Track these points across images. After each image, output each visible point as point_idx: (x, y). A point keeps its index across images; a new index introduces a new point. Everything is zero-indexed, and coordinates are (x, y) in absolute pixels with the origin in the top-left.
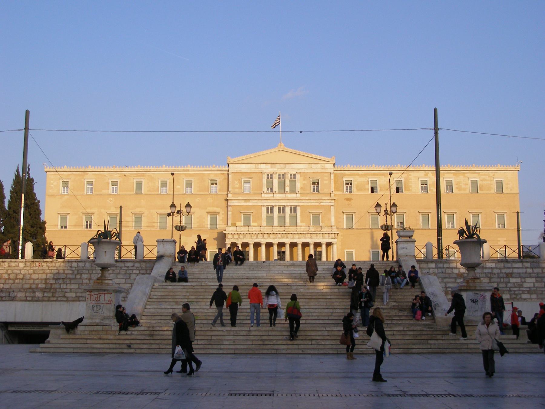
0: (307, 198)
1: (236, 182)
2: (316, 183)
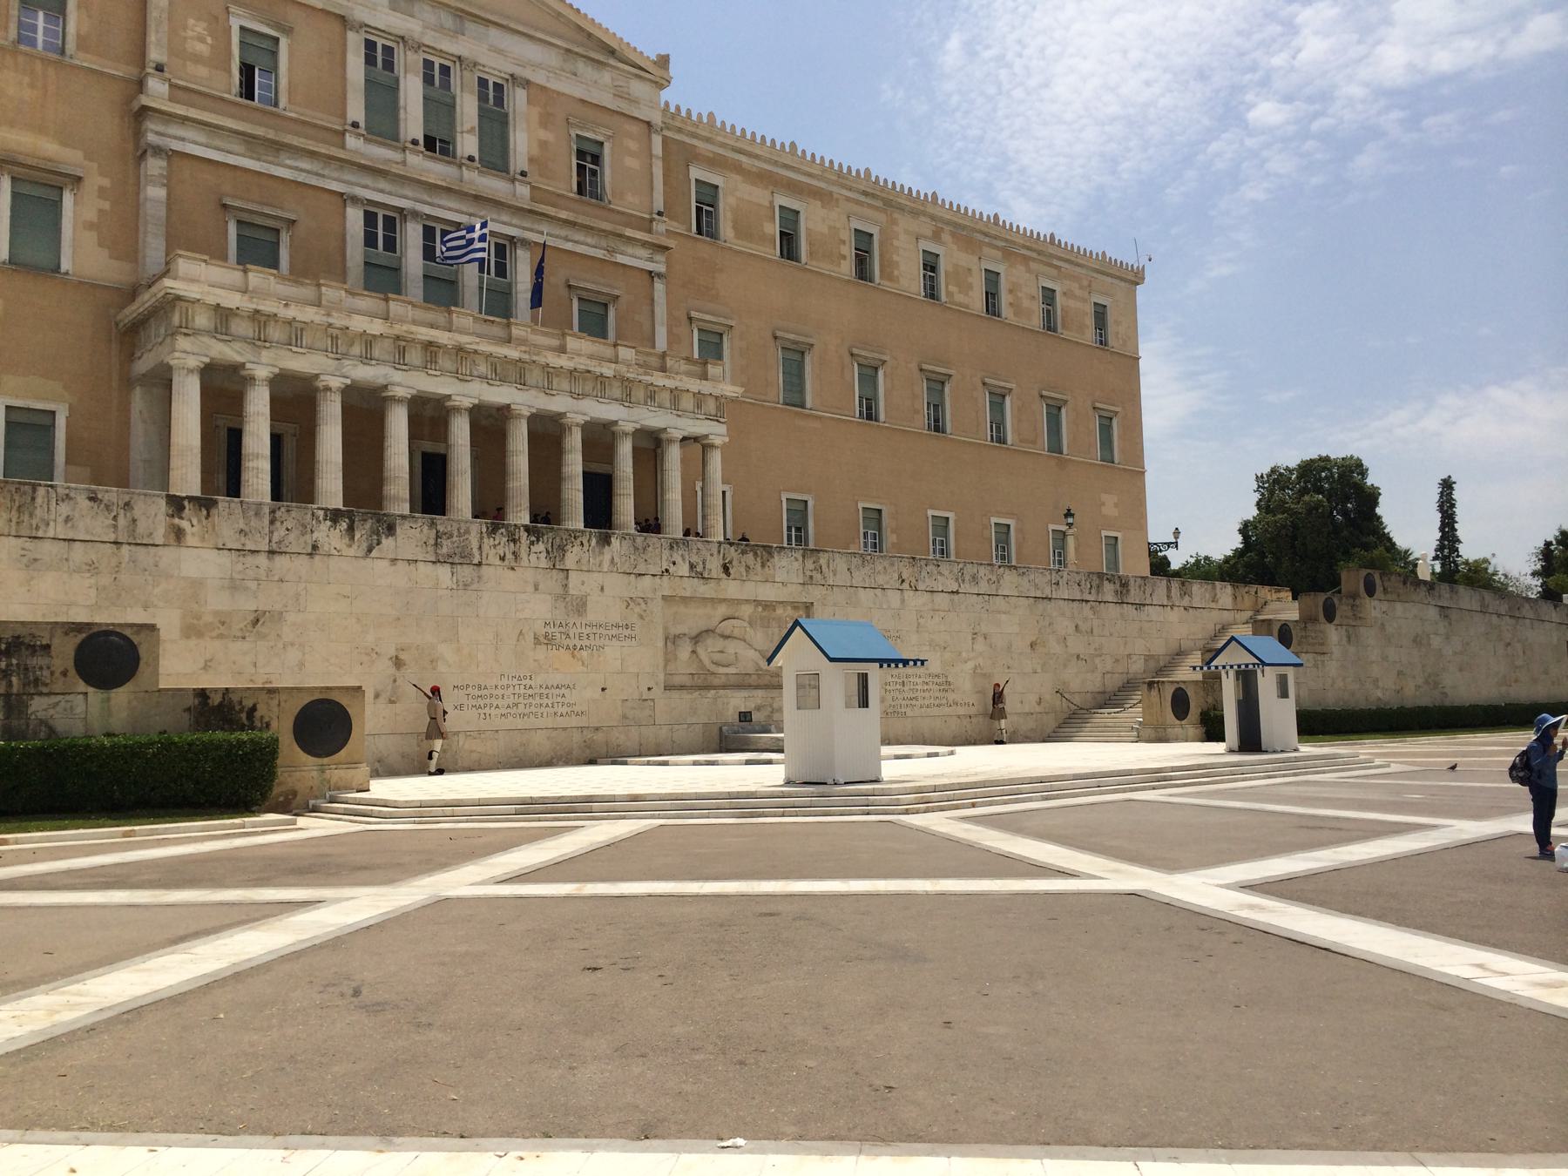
0: (563, 215)
1: (201, 28)
2: (589, 158)
